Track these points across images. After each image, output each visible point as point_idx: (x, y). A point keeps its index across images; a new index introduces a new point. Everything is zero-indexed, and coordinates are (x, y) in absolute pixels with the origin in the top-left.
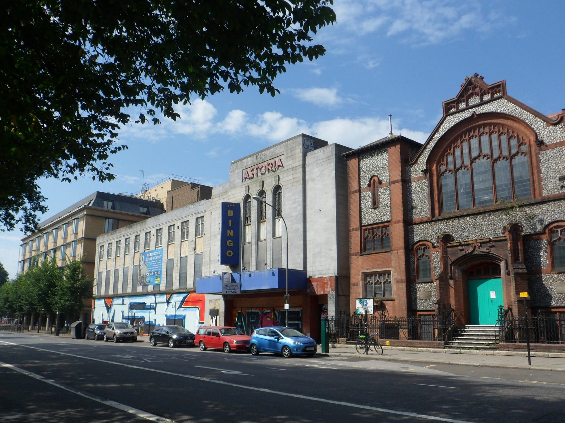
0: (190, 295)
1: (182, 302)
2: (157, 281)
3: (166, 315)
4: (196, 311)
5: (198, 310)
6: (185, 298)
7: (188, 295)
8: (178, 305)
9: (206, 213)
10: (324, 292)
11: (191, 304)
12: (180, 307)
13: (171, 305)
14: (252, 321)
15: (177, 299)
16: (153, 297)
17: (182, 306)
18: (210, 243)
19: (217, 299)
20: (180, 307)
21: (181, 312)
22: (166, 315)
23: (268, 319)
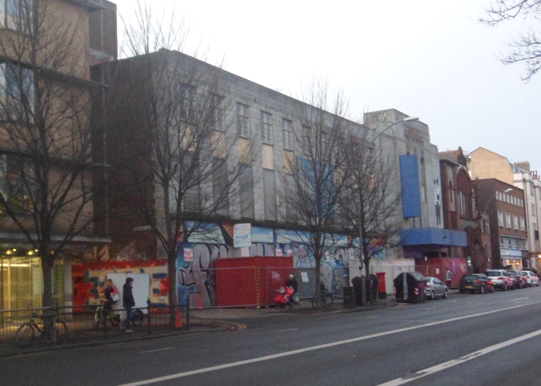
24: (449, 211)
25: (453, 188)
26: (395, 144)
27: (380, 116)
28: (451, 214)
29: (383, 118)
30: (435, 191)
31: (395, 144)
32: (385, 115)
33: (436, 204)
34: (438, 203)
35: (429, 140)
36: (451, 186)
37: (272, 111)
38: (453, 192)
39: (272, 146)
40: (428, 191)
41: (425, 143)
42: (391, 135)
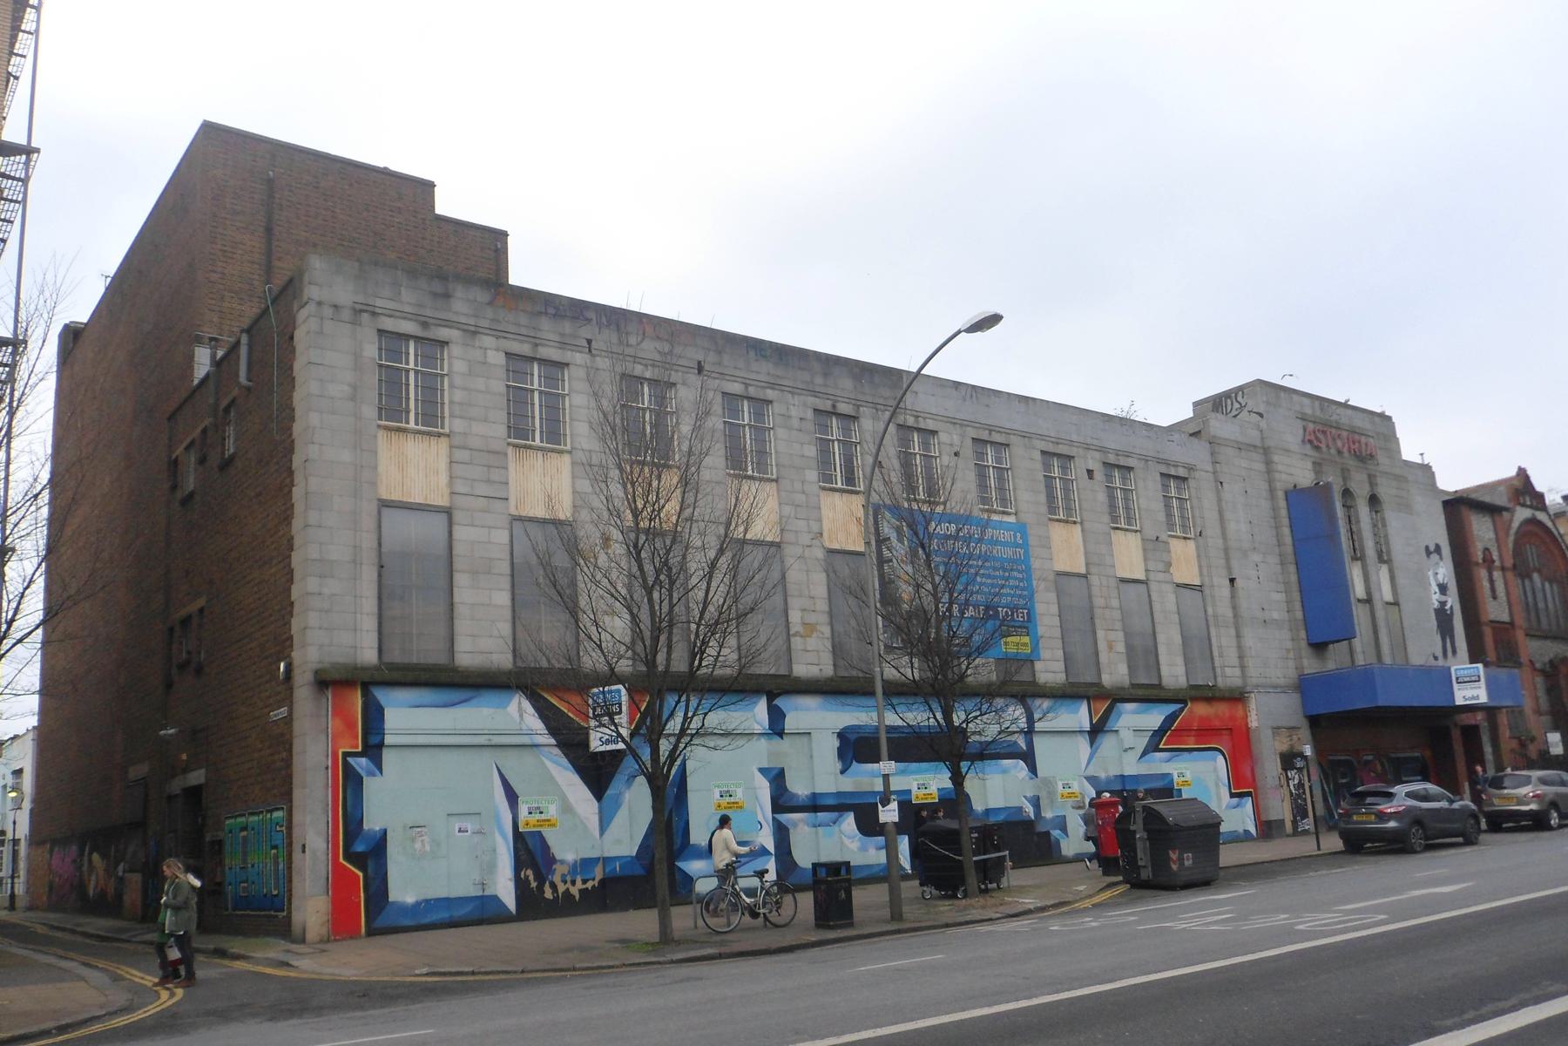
0: (1191, 711)
1: (1159, 734)
2: (1013, 644)
3: (1092, 780)
4: (1215, 760)
5: (1221, 757)
6: (1170, 719)
7: (1182, 710)
8: (1143, 742)
9: (1197, 474)
10: (1476, 720)
11: (1193, 739)
12: (1153, 747)
13: (1107, 743)
14: (1344, 781)
15: (1137, 721)
16: (1016, 712)
17: (1161, 746)
18: (1229, 568)
19: (1292, 725)
20: (1153, 747)
21: (1160, 764)
22: (1092, 780)
23: (1372, 774)
24: (1484, 619)
25: (1497, 563)
26: (1268, 463)
27: (1229, 402)
28: (1494, 629)
29: (1236, 405)
30: (1430, 573)
31: (1268, 463)
32: (1239, 399)
33: (1436, 605)
34: (1443, 604)
35: (1399, 452)
36: (1488, 561)
37: (770, 394)
38: (1497, 575)
39: (776, 481)
40: (1398, 573)
41: (1382, 458)
42: (1258, 443)
